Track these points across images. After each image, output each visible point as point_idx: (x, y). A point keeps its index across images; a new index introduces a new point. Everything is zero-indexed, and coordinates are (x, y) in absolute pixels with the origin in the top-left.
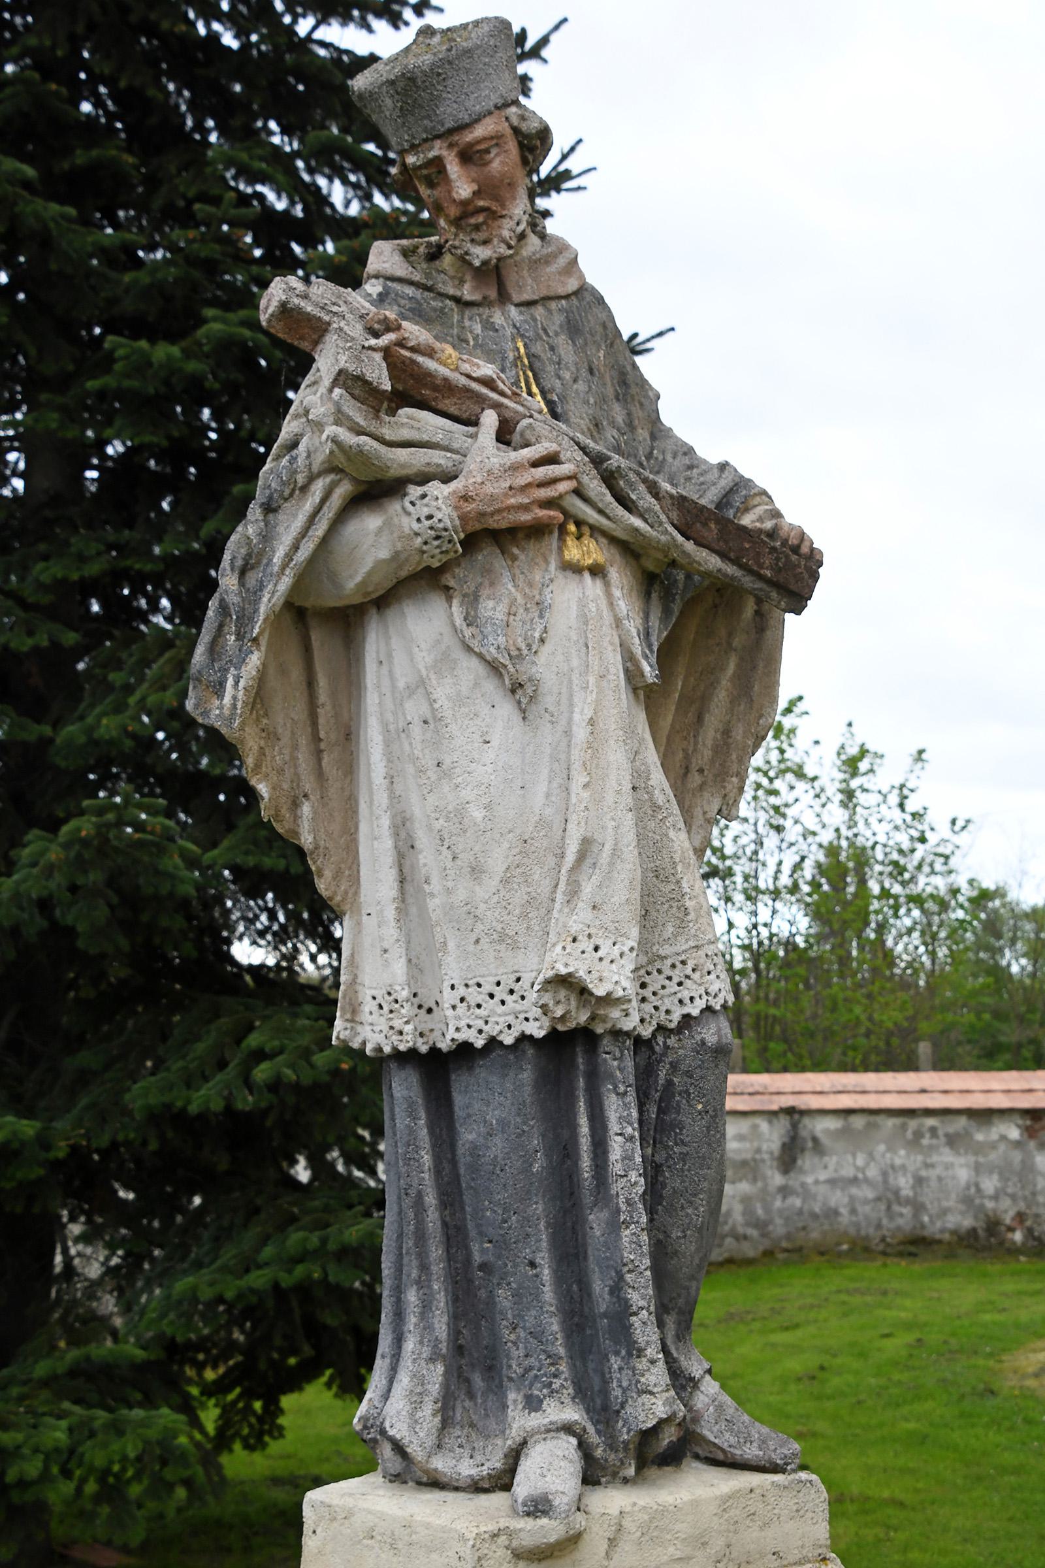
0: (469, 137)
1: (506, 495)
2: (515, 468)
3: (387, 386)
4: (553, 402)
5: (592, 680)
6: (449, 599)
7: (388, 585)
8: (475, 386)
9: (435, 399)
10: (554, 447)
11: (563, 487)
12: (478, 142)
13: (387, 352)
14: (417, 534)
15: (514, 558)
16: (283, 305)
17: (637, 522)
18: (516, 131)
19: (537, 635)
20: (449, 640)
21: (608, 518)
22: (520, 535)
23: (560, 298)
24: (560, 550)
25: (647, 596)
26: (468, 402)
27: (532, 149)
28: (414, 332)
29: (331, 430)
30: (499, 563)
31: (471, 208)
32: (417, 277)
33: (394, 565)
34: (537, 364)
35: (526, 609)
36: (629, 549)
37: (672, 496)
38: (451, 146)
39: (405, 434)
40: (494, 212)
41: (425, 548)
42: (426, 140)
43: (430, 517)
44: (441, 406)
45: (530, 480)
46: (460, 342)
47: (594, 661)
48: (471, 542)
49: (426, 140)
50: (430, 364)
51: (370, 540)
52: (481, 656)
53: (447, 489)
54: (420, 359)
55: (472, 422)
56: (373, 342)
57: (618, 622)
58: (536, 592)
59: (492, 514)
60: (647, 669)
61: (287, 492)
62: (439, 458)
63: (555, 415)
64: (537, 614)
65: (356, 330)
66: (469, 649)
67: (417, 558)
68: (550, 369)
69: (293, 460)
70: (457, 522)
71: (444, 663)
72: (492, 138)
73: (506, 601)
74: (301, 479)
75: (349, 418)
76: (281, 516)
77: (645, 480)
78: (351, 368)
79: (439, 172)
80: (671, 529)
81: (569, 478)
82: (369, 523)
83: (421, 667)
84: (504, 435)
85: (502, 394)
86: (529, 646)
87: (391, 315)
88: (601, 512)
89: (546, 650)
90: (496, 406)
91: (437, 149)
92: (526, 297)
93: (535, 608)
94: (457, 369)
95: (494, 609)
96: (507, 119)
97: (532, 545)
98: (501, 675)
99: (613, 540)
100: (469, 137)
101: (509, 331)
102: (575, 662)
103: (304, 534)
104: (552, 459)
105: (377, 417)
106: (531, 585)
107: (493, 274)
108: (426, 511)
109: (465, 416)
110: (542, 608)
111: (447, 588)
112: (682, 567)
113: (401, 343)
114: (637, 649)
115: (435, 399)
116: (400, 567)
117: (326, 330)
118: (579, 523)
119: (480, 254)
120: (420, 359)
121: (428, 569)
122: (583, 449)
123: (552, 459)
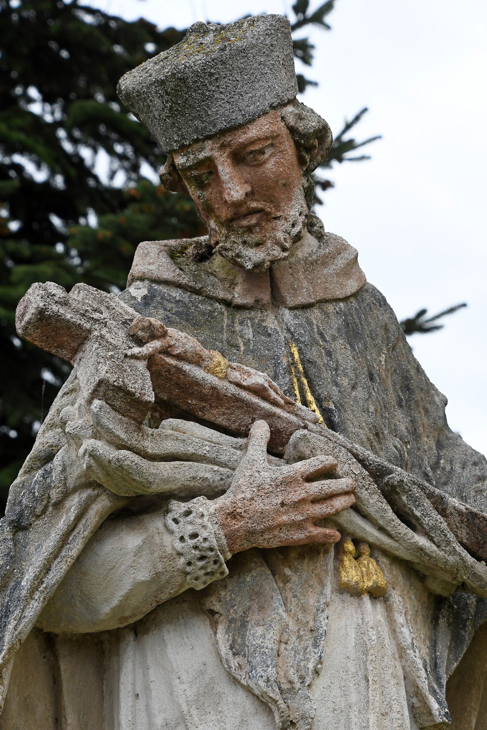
0: (242, 138)
1: (277, 512)
2: (287, 483)
3: (151, 397)
4: (330, 411)
5: (372, 718)
6: (214, 625)
7: (148, 609)
8: (244, 394)
9: (202, 409)
10: (330, 460)
11: (339, 503)
12: (252, 142)
13: (151, 361)
14: (180, 554)
15: (286, 580)
16: (41, 313)
17: (422, 541)
18: (292, 130)
19: (311, 666)
20: (213, 670)
21: (390, 535)
22: (293, 555)
23: (338, 300)
24: (337, 572)
25: (434, 621)
26: (238, 412)
27: (309, 149)
28: (182, 338)
29: (88, 443)
30: (270, 585)
31: (243, 210)
32: (185, 280)
33: (154, 587)
34: (313, 371)
35: (299, 637)
36: (414, 570)
37: (460, 513)
38: (223, 147)
39: (170, 447)
40: (269, 214)
41: (188, 569)
42: (196, 141)
43: (194, 536)
44: (208, 416)
45: (304, 495)
46: (229, 348)
47: (375, 696)
48: (239, 562)
49: (196, 141)
50: (198, 373)
51: (129, 560)
52: (248, 690)
53: (213, 505)
54: (187, 367)
55: (243, 433)
56: (136, 350)
57: (401, 652)
58: (310, 618)
59: (262, 532)
60: (435, 706)
61: (38, 510)
62: (205, 472)
63: (332, 425)
64: (310, 642)
65: (118, 337)
66: (235, 681)
67: (179, 580)
68: (327, 375)
69: (47, 474)
70: (224, 541)
71: (206, 698)
72: (267, 138)
73: (277, 627)
74: (55, 495)
75: (109, 431)
76: (32, 535)
77: (430, 496)
78: (112, 378)
79: (210, 173)
80: (459, 549)
81: (347, 493)
82: (128, 542)
83: (182, 701)
84: (276, 448)
85: (274, 403)
86: (302, 679)
87: (156, 322)
88: (381, 529)
89: (321, 683)
90: (268, 416)
91: (209, 150)
92: (301, 300)
93: (309, 635)
94: (226, 377)
95: (263, 636)
96: (283, 118)
97: (306, 566)
98: (270, 712)
99: (396, 560)
100: (242, 138)
101: (283, 336)
102: (354, 698)
103: (56, 554)
104: (328, 473)
105: (139, 429)
106: (304, 610)
107: (267, 278)
108: (190, 529)
109: (233, 427)
110: (317, 636)
111: (212, 613)
112: (473, 591)
113: (166, 351)
114: (424, 685)
115: (202, 409)
116: (161, 590)
117: (86, 338)
118: (357, 542)
119: (253, 256)
120: (187, 367)
121: (191, 591)
122: (362, 461)
123: (328, 473)
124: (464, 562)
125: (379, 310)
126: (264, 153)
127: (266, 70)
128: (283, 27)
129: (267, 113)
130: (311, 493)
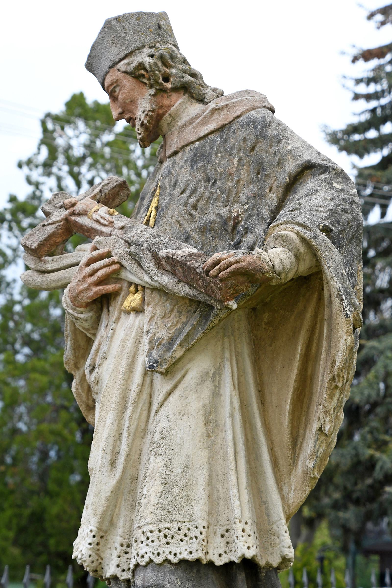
1: (78, 285)
18: (125, 72)
89: (106, 363)
96: (119, 70)
105: (41, 261)
125: (241, 131)
126: (115, 92)
127: (103, 51)
129: (108, 72)
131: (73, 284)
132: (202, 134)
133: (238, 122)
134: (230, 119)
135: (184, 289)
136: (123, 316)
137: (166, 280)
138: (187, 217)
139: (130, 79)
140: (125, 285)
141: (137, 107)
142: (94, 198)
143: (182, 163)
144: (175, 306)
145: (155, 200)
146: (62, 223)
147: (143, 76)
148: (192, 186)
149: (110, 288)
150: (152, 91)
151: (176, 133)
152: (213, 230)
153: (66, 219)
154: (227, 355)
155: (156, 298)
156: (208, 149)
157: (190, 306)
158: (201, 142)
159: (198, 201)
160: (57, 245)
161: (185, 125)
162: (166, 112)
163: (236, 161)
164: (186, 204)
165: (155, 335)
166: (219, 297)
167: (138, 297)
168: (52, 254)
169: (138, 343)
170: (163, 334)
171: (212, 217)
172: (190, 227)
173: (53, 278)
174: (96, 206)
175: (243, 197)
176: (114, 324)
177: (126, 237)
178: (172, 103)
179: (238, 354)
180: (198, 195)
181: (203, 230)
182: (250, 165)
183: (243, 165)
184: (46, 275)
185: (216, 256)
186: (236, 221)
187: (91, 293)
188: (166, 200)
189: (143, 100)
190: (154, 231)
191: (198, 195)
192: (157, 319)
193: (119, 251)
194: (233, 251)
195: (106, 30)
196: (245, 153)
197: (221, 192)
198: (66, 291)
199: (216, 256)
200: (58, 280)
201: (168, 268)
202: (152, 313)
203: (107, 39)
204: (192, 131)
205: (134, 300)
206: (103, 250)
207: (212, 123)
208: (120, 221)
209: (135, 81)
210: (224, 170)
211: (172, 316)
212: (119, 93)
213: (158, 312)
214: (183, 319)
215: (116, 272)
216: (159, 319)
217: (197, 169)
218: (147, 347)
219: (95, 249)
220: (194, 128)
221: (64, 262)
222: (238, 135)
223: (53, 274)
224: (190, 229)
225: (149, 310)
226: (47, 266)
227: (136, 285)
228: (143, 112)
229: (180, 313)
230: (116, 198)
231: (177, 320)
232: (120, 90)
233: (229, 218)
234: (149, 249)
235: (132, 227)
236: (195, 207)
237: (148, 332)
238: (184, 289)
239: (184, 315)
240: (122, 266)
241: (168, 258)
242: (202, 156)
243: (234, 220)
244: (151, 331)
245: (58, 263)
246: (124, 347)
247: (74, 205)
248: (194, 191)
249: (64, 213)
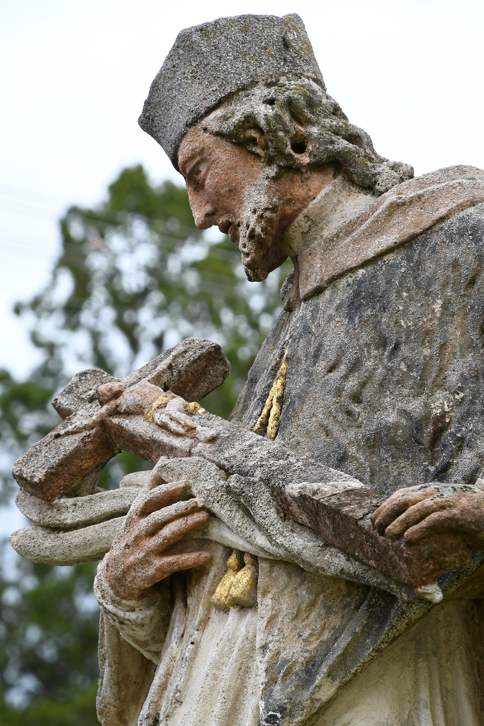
1: (124, 554)
18: (219, 134)
89: (182, 711)
96: (205, 130)
105: (51, 507)
124: (290, 552)
125: (448, 247)
126: (199, 172)
127: (175, 93)
128: (183, 41)
129: (185, 134)
130: (142, 528)
131: (115, 552)
132: (370, 253)
133: (441, 229)
134: (426, 224)
135: (336, 562)
136: (214, 616)
137: (300, 543)
138: (340, 417)
139: (228, 147)
140: (219, 553)
141: (242, 202)
142: (156, 380)
143: (331, 312)
144: (317, 595)
145: (277, 384)
146: (93, 431)
147: (253, 141)
148: (350, 355)
149: (188, 558)
150: (272, 171)
151: (320, 251)
152: (392, 442)
153: (102, 424)
154: (424, 694)
155: (280, 580)
156: (383, 283)
157: (349, 595)
158: (369, 268)
159: (363, 385)
160: (83, 474)
161: (337, 235)
162: (300, 210)
163: (437, 306)
164: (339, 391)
165: (278, 653)
166: (405, 577)
167: (244, 577)
168: (74, 493)
169: (243, 670)
170: (295, 651)
171: (391, 418)
172: (348, 437)
173: (76, 541)
174: (161, 396)
175: (453, 378)
176: (196, 632)
177: (221, 458)
178: (311, 193)
179: (447, 695)
180: (363, 373)
181: (374, 442)
182: (466, 314)
183: (453, 315)
184: (61, 535)
185: (398, 495)
186: (440, 425)
187: (151, 571)
188: (298, 384)
189: (253, 188)
190: (276, 445)
191: (363, 373)
192: (282, 621)
193: (206, 485)
194: (432, 486)
195: (181, 52)
196: (457, 291)
197: (408, 367)
198: (101, 566)
199: (398, 495)
200: (86, 544)
201: (304, 518)
202: (273, 609)
203: (183, 70)
204: (351, 248)
205: (236, 583)
206: (174, 484)
207: (390, 231)
208: (209, 425)
209: (237, 151)
210: (415, 325)
211: (312, 616)
212: (206, 175)
213: (284, 606)
214: (335, 621)
215: (201, 528)
216: (286, 621)
217: (360, 322)
218: (262, 678)
219: (159, 481)
220: (355, 241)
221: (97, 508)
222: (442, 256)
223: (75, 533)
224: (347, 441)
225: (265, 604)
226: (63, 517)
227: (241, 554)
228: (254, 212)
229: (329, 610)
230: (203, 379)
231: (322, 623)
232: (208, 170)
233: (426, 418)
234: (266, 481)
235: (231, 439)
236: (356, 398)
237: (264, 648)
238: (336, 562)
239: (336, 613)
240: (212, 515)
241: (303, 499)
242: (372, 298)
243: (435, 424)
244: (271, 646)
245: (87, 510)
246: (216, 680)
247: (117, 394)
248: (355, 366)
249: (98, 412)
